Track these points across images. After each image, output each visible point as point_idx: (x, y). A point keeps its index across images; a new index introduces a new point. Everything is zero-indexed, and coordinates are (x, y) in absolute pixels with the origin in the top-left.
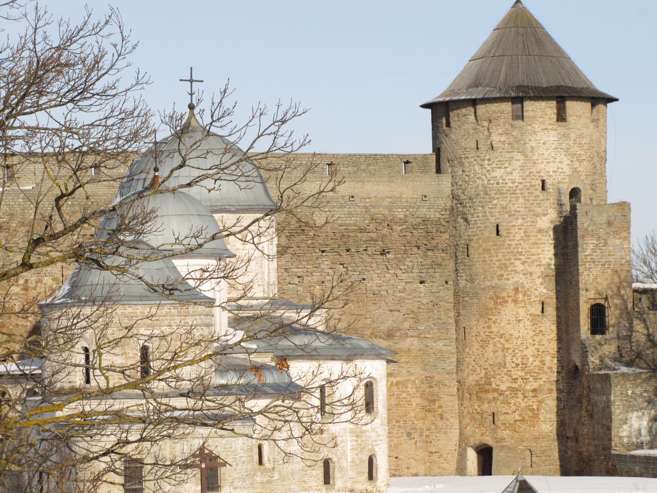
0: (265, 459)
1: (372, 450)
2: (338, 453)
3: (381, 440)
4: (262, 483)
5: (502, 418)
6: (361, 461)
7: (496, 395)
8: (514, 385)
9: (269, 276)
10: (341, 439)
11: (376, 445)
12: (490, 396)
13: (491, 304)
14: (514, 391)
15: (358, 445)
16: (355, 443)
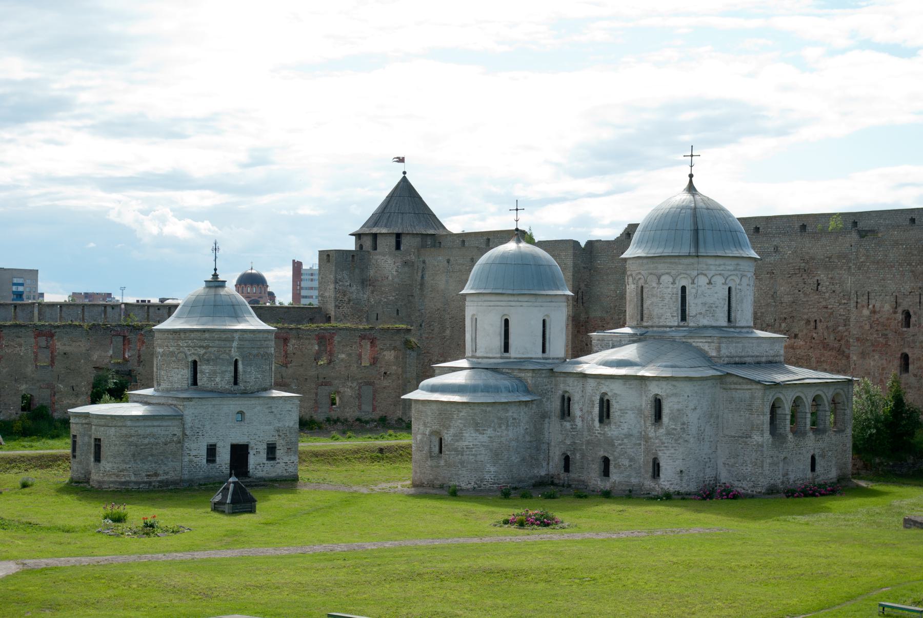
1: (656, 454)
4: (431, 466)
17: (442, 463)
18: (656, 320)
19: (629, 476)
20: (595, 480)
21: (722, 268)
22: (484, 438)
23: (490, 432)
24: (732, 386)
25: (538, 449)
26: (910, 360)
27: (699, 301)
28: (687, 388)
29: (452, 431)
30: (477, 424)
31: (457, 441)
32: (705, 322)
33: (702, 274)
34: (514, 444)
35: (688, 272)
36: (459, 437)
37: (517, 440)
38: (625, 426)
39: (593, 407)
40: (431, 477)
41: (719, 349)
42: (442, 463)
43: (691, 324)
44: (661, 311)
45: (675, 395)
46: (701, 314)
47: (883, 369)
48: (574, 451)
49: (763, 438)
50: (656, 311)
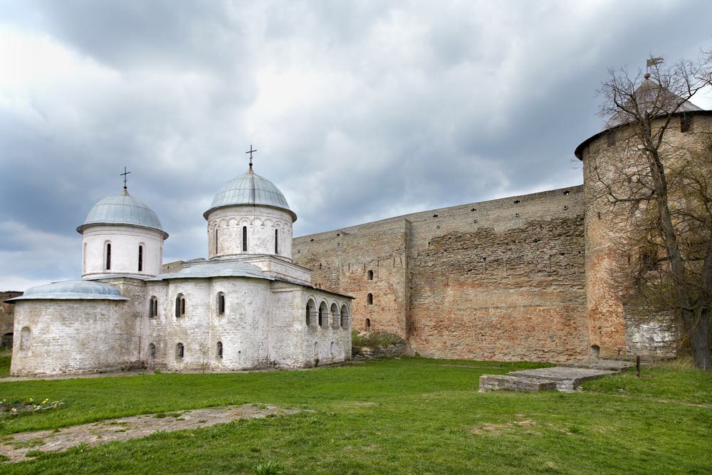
4: (20, 358)
5: (604, 329)
7: (601, 316)
8: (610, 309)
12: (598, 316)
13: (596, 261)
14: (611, 312)
18: (226, 251)
19: (199, 358)
20: (173, 363)
21: (271, 215)
22: (71, 331)
23: (77, 325)
24: (279, 290)
25: (129, 340)
26: (373, 297)
27: (256, 237)
28: (244, 287)
29: (40, 326)
30: (64, 319)
32: (260, 251)
33: (258, 218)
34: (102, 335)
36: (45, 330)
37: (106, 332)
41: (269, 266)
42: (30, 354)
43: (250, 253)
45: (235, 291)
47: (358, 303)
48: (159, 342)
49: (300, 326)
50: (226, 245)
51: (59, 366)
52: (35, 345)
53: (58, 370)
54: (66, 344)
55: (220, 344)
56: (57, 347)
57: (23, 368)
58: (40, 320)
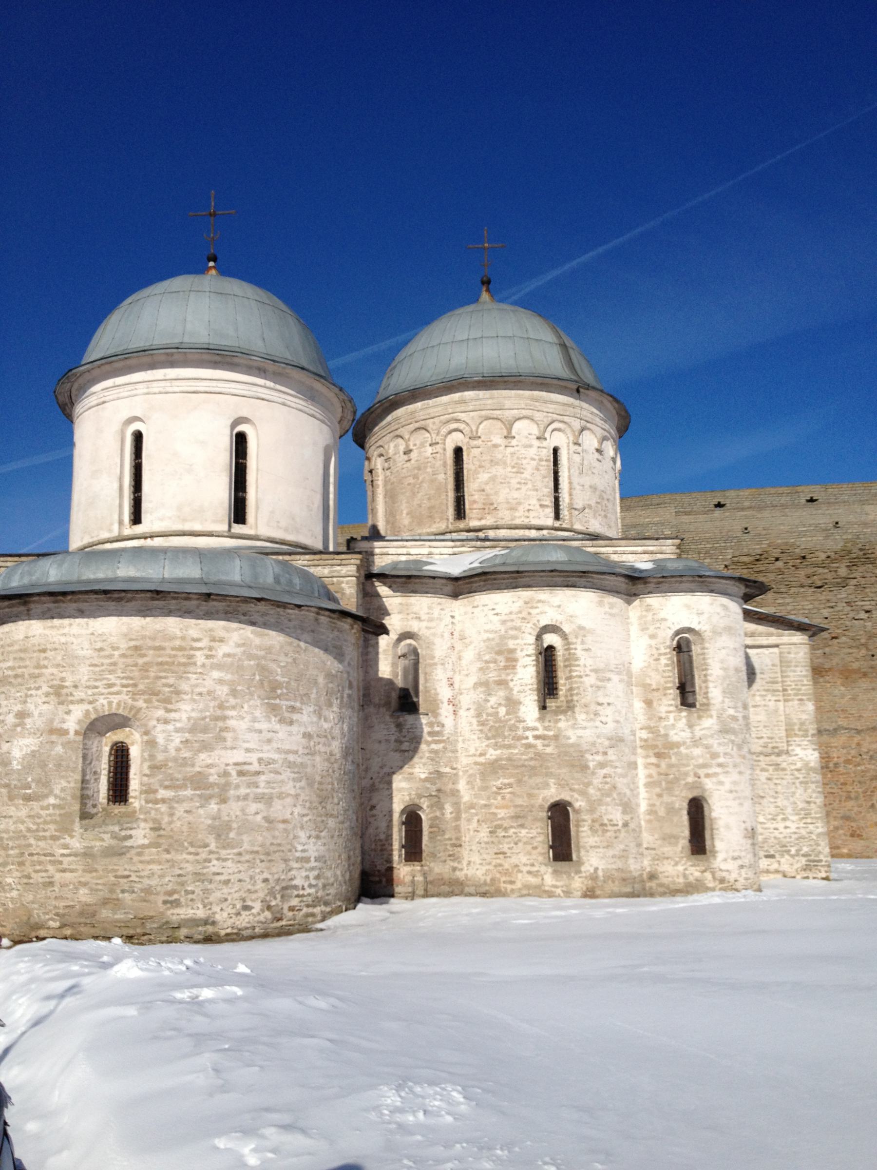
0: (135, 784)
1: (698, 785)
2: (591, 790)
3: (720, 765)
4: (87, 854)
6: (671, 810)
9: (570, 495)
10: (599, 758)
11: (707, 776)
15: (660, 774)
16: (653, 771)
17: (141, 835)
19: (624, 856)
29: (186, 711)
30: (274, 686)
31: (206, 747)
35: (566, 419)
36: (209, 731)
38: (608, 713)
39: (511, 662)
40: (84, 895)
44: (516, 494)
46: (590, 507)
48: (437, 798)
50: (503, 496)
51: (262, 890)
52: (162, 793)
53: (257, 906)
54: (281, 796)
55: (697, 810)
56: (254, 807)
57: (105, 902)
58: (184, 686)
